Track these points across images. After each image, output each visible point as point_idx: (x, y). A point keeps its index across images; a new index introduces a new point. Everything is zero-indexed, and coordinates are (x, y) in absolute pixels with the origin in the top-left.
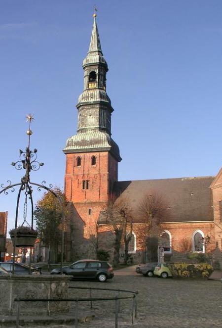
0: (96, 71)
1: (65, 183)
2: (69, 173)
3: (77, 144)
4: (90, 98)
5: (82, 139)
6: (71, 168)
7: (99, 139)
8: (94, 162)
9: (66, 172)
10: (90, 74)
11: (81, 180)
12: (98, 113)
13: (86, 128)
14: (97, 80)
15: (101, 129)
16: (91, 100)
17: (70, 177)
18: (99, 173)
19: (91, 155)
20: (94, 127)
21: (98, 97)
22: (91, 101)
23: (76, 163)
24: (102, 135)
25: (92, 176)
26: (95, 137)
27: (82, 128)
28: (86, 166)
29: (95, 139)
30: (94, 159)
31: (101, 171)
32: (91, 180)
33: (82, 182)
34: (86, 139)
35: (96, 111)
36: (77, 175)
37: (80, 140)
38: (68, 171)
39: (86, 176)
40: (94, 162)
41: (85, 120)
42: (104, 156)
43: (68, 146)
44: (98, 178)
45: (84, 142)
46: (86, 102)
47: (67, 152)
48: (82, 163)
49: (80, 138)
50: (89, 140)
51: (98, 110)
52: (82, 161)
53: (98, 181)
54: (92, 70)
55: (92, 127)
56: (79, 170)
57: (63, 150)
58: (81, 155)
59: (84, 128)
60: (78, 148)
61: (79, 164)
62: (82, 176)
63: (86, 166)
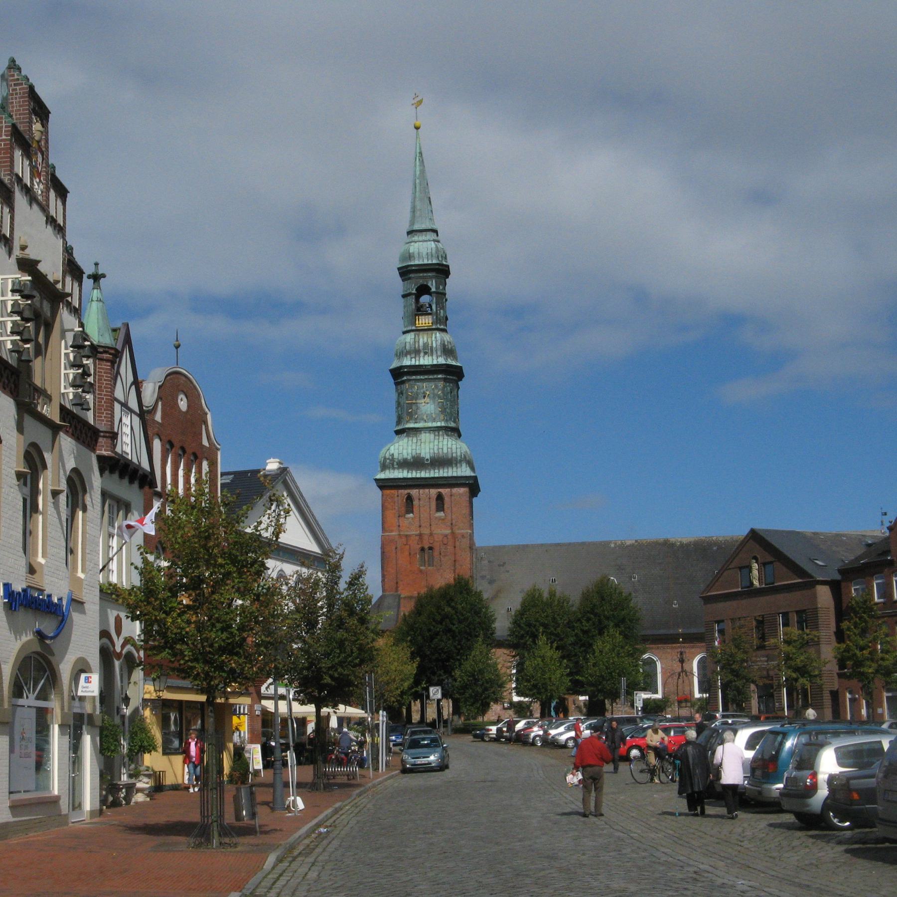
0: (429, 284)
3: (404, 464)
4: (422, 354)
5: (414, 454)
18: (453, 533)
19: (434, 492)
22: (426, 363)
24: (454, 447)
30: (440, 498)
32: (436, 546)
34: (423, 455)
35: (436, 387)
36: (407, 536)
39: (426, 537)
45: (417, 463)
46: (415, 366)
47: (383, 485)
49: (410, 451)
50: (428, 457)
52: (416, 503)
53: (450, 548)
54: (421, 282)
56: (410, 523)
57: (376, 480)
58: (414, 492)
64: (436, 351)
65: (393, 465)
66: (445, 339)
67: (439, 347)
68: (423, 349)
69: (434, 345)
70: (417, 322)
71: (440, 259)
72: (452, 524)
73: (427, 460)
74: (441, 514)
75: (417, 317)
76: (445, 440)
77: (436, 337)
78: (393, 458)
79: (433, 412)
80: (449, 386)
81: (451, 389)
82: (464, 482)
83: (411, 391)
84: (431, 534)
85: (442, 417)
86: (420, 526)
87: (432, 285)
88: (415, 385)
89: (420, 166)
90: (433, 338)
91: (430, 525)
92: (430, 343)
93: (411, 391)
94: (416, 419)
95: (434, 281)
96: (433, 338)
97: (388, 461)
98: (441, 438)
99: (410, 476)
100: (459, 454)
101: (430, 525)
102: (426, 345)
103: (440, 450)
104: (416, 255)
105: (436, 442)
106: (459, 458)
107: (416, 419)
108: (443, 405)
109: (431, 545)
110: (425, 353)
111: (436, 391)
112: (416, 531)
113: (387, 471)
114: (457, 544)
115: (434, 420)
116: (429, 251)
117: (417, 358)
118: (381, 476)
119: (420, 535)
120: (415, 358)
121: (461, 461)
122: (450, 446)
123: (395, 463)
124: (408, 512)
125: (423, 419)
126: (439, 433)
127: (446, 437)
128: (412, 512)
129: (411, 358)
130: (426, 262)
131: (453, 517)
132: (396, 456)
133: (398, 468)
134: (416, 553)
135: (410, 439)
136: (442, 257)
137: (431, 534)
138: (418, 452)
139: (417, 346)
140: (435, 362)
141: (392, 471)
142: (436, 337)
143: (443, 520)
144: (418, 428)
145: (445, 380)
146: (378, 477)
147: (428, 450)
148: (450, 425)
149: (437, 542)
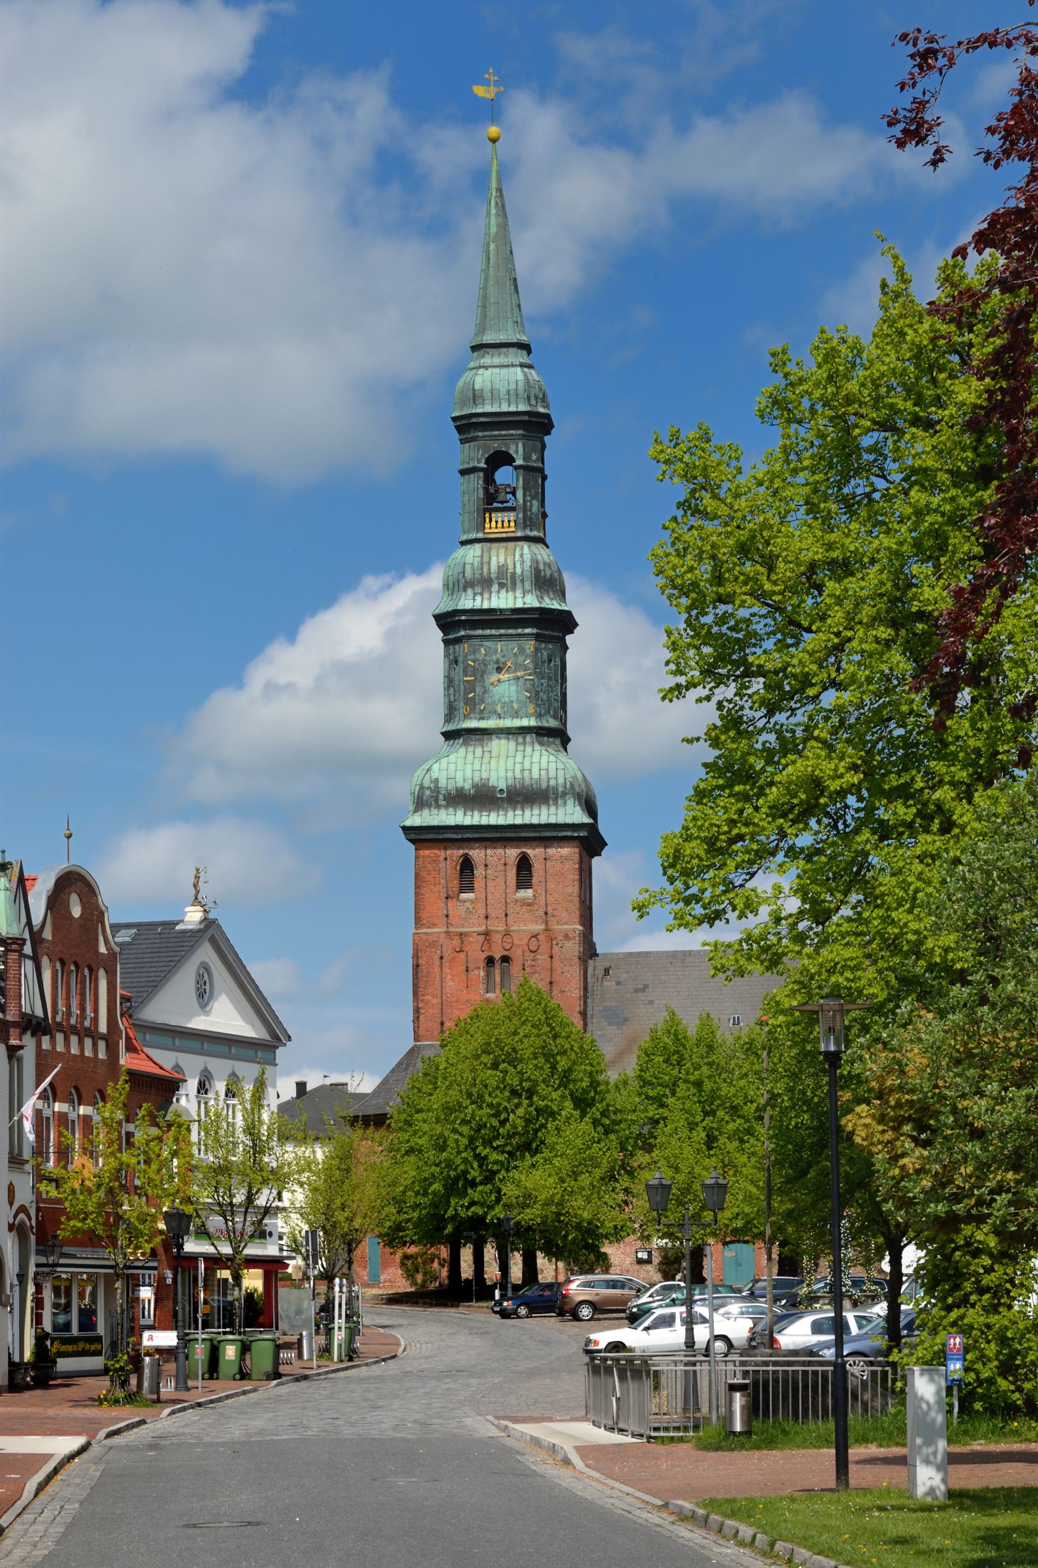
0: (512, 452)
1: (416, 967)
2: (434, 925)
3: (459, 798)
5: (477, 779)
6: (433, 895)
9: (418, 920)
16: (502, 600)
17: (433, 944)
18: (547, 930)
24: (552, 766)
25: (520, 941)
26: (526, 773)
29: (527, 782)
30: (524, 865)
31: (552, 922)
35: (522, 650)
37: (467, 786)
38: (424, 915)
39: (497, 938)
41: (478, 690)
42: (563, 859)
43: (420, 803)
44: (544, 948)
47: (419, 837)
48: (478, 883)
49: (469, 774)
50: (502, 785)
51: (530, 645)
57: (405, 829)
64: (522, 581)
65: (437, 801)
66: (539, 557)
67: (527, 574)
68: (498, 578)
69: (519, 571)
70: (487, 525)
71: (533, 402)
72: (546, 913)
73: (502, 791)
75: (487, 515)
76: (536, 754)
77: (522, 555)
78: (437, 787)
79: (514, 699)
80: (545, 649)
83: (472, 657)
84: (507, 933)
85: (531, 708)
86: (487, 917)
87: (517, 452)
88: (482, 646)
89: (497, 215)
90: (517, 557)
91: (506, 915)
92: (510, 566)
93: (472, 657)
94: (482, 711)
95: (520, 445)
96: (517, 557)
97: (428, 792)
98: (529, 749)
99: (468, 821)
100: (561, 781)
101: (506, 915)
102: (502, 569)
103: (526, 773)
104: (487, 394)
105: (519, 755)
106: (561, 789)
108: (533, 685)
109: (506, 953)
110: (502, 586)
111: (520, 659)
112: (479, 925)
113: (426, 812)
114: (556, 949)
115: (516, 715)
116: (512, 386)
117: (486, 596)
118: (416, 820)
119: (487, 934)
120: (482, 594)
121: (564, 794)
122: (544, 765)
123: (441, 797)
124: (462, 890)
125: (495, 712)
126: (524, 739)
127: (537, 747)
128: (471, 889)
129: (475, 595)
130: (505, 408)
131: (550, 899)
132: (443, 783)
133: (447, 807)
135: (471, 749)
136: (536, 398)
137: (507, 933)
138: (485, 775)
139: (485, 570)
140: (519, 605)
141: (434, 811)
142: (522, 555)
143: (529, 905)
145: (538, 637)
146: (408, 823)
147: (502, 774)
148: (546, 724)
149: (518, 946)
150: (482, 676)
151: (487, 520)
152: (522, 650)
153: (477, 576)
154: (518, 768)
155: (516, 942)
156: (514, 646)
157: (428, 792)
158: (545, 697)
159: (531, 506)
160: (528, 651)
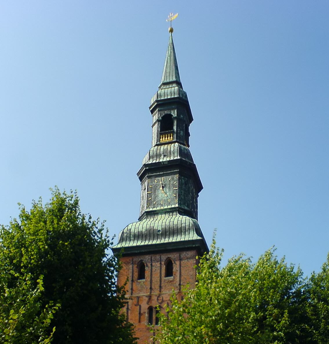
0: (172, 114)
3: (139, 236)
7: (179, 226)
8: (169, 272)
10: (162, 118)
11: (145, 306)
12: (176, 183)
13: (155, 209)
14: (175, 128)
15: (181, 211)
19: (164, 257)
20: (169, 207)
21: (176, 154)
23: (136, 275)
27: (148, 210)
28: (156, 278)
33: (147, 311)
35: (173, 179)
36: (138, 298)
40: (169, 272)
45: (151, 234)
48: (147, 274)
51: (176, 177)
54: (166, 112)
55: (166, 207)
59: (151, 209)
60: (140, 243)
61: (141, 276)
62: (147, 299)
63: (156, 278)
65: (130, 238)
69: (172, 149)
70: (161, 139)
73: (159, 231)
74: (171, 278)
75: (161, 136)
76: (177, 218)
81: (185, 182)
82: (191, 246)
88: (155, 179)
94: (154, 205)
97: (125, 235)
99: (143, 244)
100: (187, 224)
106: (187, 227)
107: (154, 205)
110: (164, 156)
123: (132, 236)
132: (132, 230)
134: (145, 313)
139: (158, 151)
143: (171, 282)
144: (155, 211)
150: (155, 191)
151: (161, 138)
152: (173, 179)
153: (155, 154)
154: (168, 221)
155: (164, 299)
156: (170, 178)
157: (125, 235)
158: (183, 198)
159: (180, 133)
160: (175, 179)
